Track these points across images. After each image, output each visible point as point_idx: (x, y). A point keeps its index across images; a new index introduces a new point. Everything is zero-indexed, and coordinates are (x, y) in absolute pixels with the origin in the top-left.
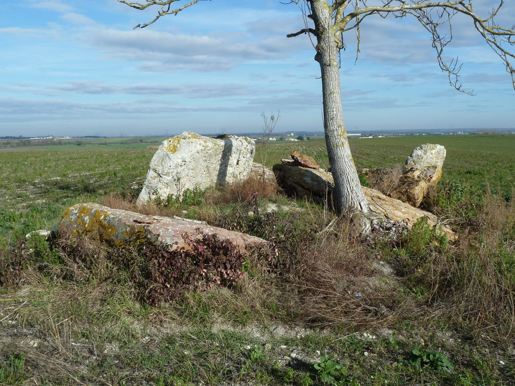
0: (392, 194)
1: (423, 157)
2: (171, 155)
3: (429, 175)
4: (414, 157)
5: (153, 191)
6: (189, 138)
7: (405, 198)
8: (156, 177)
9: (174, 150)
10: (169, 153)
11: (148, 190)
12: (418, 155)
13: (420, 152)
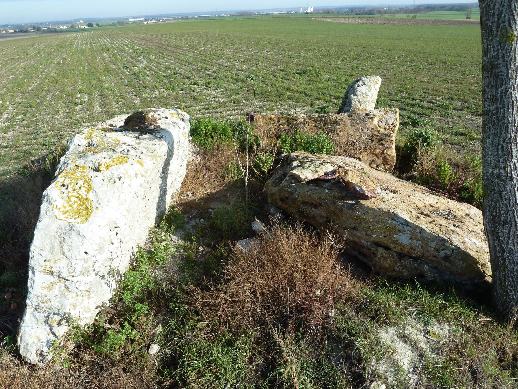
0: (361, 157)
1: (367, 96)
2: (84, 227)
3: (390, 123)
4: (359, 96)
5: (58, 318)
6: (107, 167)
7: (379, 161)
8: (55, 283)
9: (85, 210)
10: (72, 221)
11: (41, 317)
12: (363, 94)
13: (365, 89)
